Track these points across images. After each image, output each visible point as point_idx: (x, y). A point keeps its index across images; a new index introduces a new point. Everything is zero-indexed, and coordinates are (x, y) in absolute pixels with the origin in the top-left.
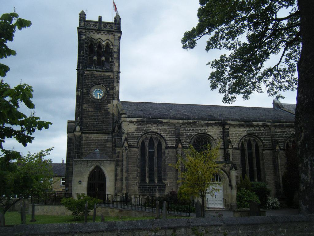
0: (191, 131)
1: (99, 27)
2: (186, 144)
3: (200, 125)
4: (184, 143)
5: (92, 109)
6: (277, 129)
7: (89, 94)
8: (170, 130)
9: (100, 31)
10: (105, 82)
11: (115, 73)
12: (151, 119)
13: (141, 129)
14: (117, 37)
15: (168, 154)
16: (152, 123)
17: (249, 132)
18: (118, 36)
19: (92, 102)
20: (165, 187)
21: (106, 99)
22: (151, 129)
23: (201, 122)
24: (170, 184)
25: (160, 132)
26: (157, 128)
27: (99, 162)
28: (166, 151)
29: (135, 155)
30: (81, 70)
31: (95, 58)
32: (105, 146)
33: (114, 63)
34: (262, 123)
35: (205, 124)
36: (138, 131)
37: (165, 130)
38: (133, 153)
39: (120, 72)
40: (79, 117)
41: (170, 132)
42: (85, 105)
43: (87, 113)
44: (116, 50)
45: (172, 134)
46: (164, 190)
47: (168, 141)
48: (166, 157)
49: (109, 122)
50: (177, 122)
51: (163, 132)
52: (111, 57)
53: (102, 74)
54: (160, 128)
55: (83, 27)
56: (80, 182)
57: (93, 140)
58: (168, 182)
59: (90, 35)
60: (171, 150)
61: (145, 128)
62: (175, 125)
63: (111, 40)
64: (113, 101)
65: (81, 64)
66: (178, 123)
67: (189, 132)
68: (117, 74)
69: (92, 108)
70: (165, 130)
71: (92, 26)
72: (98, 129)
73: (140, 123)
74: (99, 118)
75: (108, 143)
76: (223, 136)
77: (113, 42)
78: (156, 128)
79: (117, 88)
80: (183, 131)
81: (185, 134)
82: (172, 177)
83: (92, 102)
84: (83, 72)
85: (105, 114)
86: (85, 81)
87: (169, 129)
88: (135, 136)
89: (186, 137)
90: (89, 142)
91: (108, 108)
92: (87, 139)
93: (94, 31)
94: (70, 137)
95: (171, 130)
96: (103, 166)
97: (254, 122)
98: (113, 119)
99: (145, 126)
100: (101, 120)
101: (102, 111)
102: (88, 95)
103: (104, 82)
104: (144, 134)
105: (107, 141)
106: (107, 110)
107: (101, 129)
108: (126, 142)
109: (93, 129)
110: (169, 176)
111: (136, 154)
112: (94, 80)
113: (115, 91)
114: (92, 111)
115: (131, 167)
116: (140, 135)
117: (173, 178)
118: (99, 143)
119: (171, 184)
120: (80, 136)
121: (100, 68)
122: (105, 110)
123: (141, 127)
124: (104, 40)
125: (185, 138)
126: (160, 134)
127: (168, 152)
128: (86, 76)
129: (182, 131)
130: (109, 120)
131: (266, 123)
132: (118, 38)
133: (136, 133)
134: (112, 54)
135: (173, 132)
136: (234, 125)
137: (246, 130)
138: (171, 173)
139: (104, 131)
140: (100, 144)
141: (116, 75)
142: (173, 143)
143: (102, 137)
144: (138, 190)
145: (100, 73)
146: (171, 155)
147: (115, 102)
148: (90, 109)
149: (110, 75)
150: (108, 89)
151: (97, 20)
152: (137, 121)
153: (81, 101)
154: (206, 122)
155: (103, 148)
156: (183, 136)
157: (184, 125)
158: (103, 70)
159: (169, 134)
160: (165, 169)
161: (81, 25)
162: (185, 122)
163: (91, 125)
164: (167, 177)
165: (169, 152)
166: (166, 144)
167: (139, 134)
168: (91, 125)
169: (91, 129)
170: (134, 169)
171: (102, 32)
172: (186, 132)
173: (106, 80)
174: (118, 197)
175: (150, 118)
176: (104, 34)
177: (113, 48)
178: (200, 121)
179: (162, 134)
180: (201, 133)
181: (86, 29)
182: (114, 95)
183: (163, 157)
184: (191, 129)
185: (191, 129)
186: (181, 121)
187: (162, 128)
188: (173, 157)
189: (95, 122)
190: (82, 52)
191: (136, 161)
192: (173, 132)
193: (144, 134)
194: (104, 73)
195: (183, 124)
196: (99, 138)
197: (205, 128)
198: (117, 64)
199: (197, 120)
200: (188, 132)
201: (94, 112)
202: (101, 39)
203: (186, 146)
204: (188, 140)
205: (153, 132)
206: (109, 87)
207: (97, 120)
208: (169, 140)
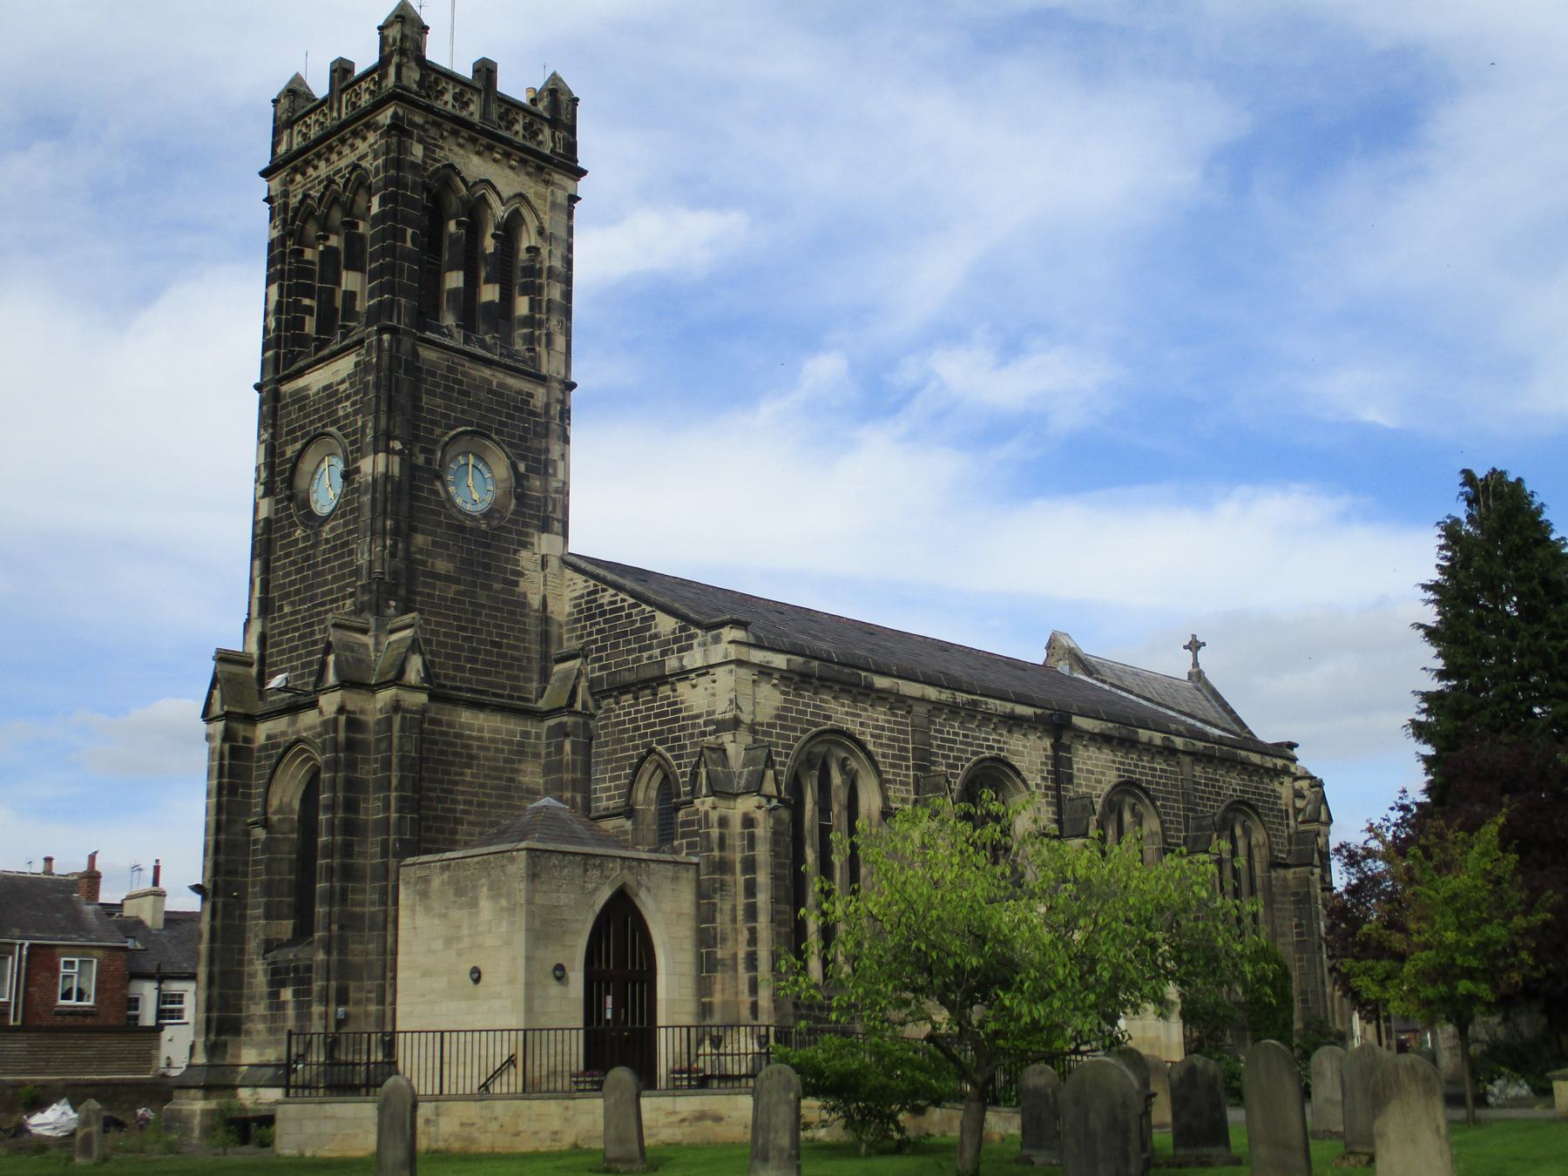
0: (962, 743)
1: (485, 115)
3: (987, 717)
5: (451, 566)
6: (1198, 770)
7: (439, 477)
8: (892, 730)
9: (487, 139)
10: (504, 424)
11: (555, 385)
12: (836, 667)
13: (798, 712)
14: (561, 197)
16: (837, 687)
17: (1125, 771)
18: (564, 188)
19: (450, 526)
21: (508, 522)
22: (828, 718)
23: (996, 705)
27: (630, 868)
30: (406, 333)
31: (454, 280)
32: (511, 780)
33: (549, 335)
34: (1163, 735)
36: (784, 718)
37: (875, 727)
39: (573, 386)
40: (393, 603)
42: (419, 539)
43: (426, 585)
44: (557, 263)
45: (901, 749)
49: (526, 649)
51: (872, 736)
52: (525, 291)
53: (495, 377)
54: (859, 716)
55: (416, 94)
56: (558, 973)
57: (459, 741)
59: (442, 148)
61: (808, 705)
63: (531, 197)
64: (540, 539)
65: (403, 301)
67: (951, 749)
68: (564, 394)
69: (451, 558)
70: (875, 727)
71: (448, 97)
72: (478, 682)
73: (797, 679)
74: (482, 623)
75: (523, 767)
76: (1057, 781)
77: (546, 218)
78: (847, 714)
79: (560, 465)
80: (936, 738)
81: (946, 757)
83: (450, 526)
84: (413, 345)
85: (505, 602)
86: (420, 399)
88: (777, 745)
90: (442, 752)
91: (521, 574)
92: (433, 732)
93: (465, 133)
94: (354, 712)
95: (900, 732)
96: (648, 889)
97: (1140, 730)
98: (545, 638)
100: (490, 634)
101: (497, 586)
102: (433, 484)
103: (502, 424)
104: (811, 738)
105: (520, 751)
106: (516, 584)
107: (490, 684)
108: (770, 773)
109: (454, 678)
112: (458, 402)
113: (555, 484)
114: (448, 579)
116: (796, 739)
118: (486, 758)
120: (424, 710)
121: (483, 345)
122: (506, 581)
123: (797, 703)
124: (505, 195)
126: (861, 745)
128: (420, 369)
130: (523, 641)
131: (1172, 737)
132: (566, 203)
133: (782, 727)
134: (538, 281)
136: (1087, 732)
137: (1114, 762)
139: (501, 696)
140: (490, 768)
141: (558, 401)
142: (904, 795)
143: (497, 731)
145: (487, 372)
147: (546, 543)
148: (442, 566)
149: (531, 395)
150: (522, 467)
151: (467, 72)
152: (789, 671)
153: (404, 508)
154: (1008, 706)
155: (508, 789)
158: (496, 358)
159: (888, 746)
161: (405, 82)
163: (448, 656)
167: (787, 737)
168: (448, 656)
169: (447, 677)
171: (500, 147)
172: (942, 747)
174: (725, 1055)
175: (833, 662)
176: (505, 161)
177: (544, 252)
178: (990, 700)
179: (871, 747)
181: (429, 109)
182: (550, 508)
186: (932, 693)
187: (869, 718)
189: (464, 638)
190: (409, 231)
194: (501, 376)
195: (937, 706)
196: (486, 735)
197: (1001, 735)
198: (559, 342)
199: (979, 695)
201: (457, 581)
202: (494, 188)
206: (523, 458)
207: (475, 630)
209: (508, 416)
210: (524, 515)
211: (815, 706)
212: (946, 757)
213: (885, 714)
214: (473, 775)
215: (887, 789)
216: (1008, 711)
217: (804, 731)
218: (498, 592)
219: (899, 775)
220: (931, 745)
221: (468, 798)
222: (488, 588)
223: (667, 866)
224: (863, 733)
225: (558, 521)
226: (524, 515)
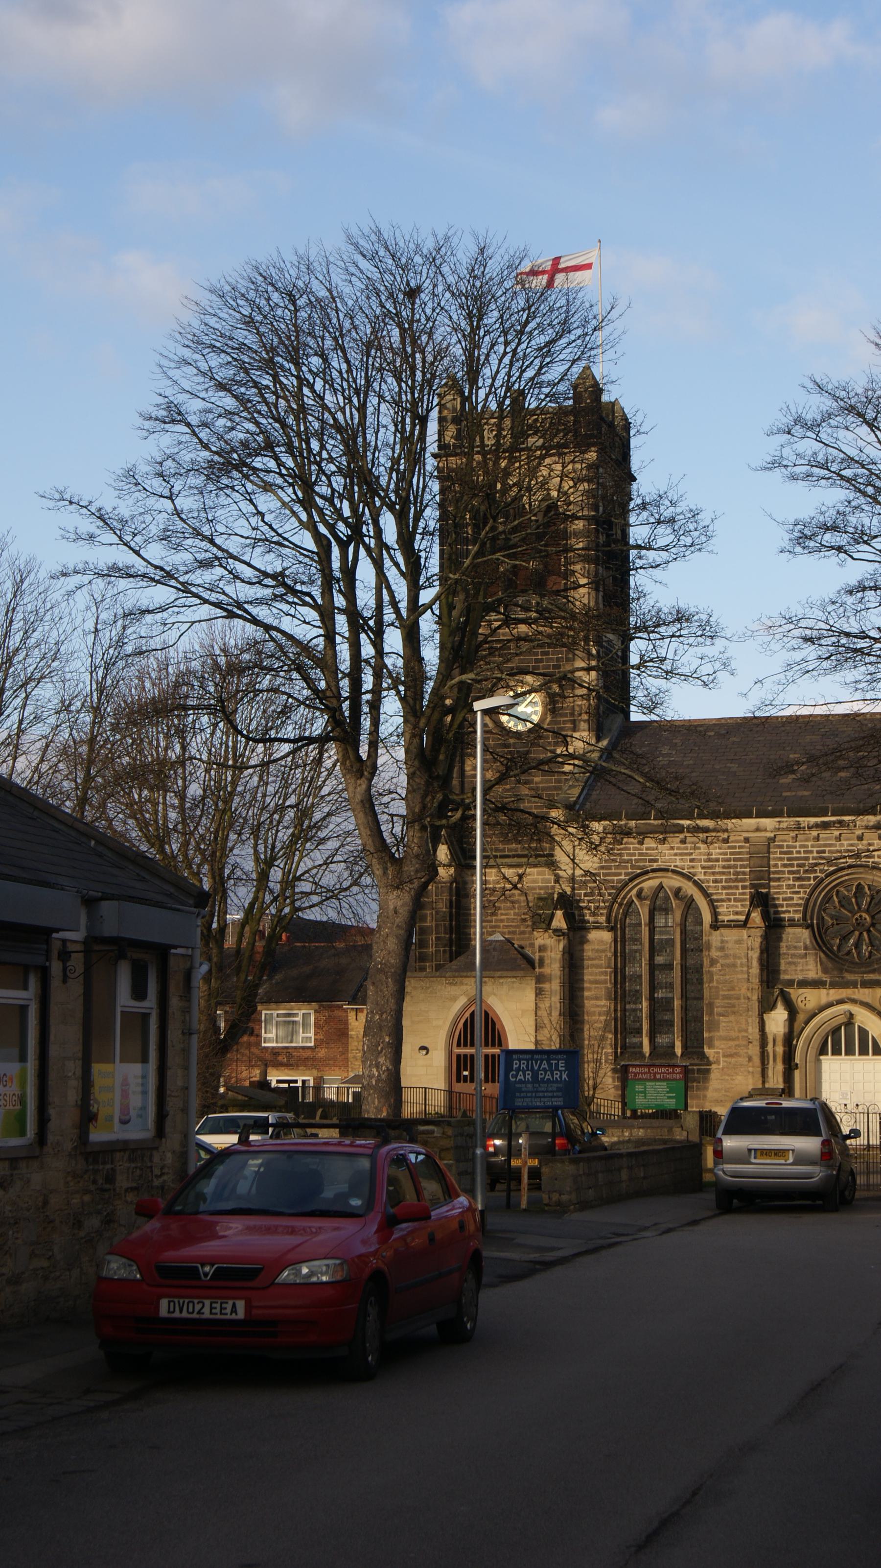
0: (814, 858)
2: (789, 912)
4: (782, 906)
8: (729, 860)
10: (541, 661)
15: (722, 949)
20: (708, 1071)
22: (656, 861)
24: (726, 1059)
25: (692, 870)
26: (681, 854)
28: (715, 938)
29: (600, 957)
35: (867, 827)
38: (593, 950)
41: (729, 867)
45: (737, 873)
46: (706, 1080)
47: (722, 900)
48: (713, 962)
50: (754, 827)
51: (703, 868)
54: (691, 854)
58: (718, 1053)
60: (730, 935)
61: (634, 855)
62: (747, 840)
66: (758, 830)
70: (709, 860)
78: (676, 855)
80: (781, 859)
81: (790, 872)
82: (733, 1034)
87: (726, 854)
89: (791, 882)
95: (735, 860)
99: (635, 849)
104: (631, 880)
109: (503, 850)
110: (722, 1033)
111: (604, 951)
115: (588, 998)
116: (619, 881)
117: (737, 1038)
119: (733, 1060)
125: (789, 887)
126: (688, 877)
127: (722, 942)
129: (777, 861)
135: (742, 866)
138: (732, 1018)
142: (740, 909)
144: (610, 1080)
146: (731, 952)
156: (778, 879)
157: (786, 837)
159: (723, 873)
160: (711, 1005)
162: (784, 825)
164: (717, 1034)
165: (727, 942)
166: (715, 914)
170: (598, 1006)
172: (792, 865)
173: (547, 653)
180: (850, 867)
183: (706, 962)
184: (811, 852)
185: (811, 852)
188: (739, 962)
191: (603, 977)
192: (742, 866)
193: (631, 880)
199: (833, 815)
200: (798, 865)
203: (791, 920)
204: (798, 893)
205: (666, 870)
208: (724, 897)
209: (543, 654)
210: (559, 723)
211: (640, 854)
212: (790, 872)
213: (720, 848)
214: (515, 914)
215: (717, 907)
216: (871, 824)
217: (626, 874)
218: (540, 783)
219: (735, 894)
220: (776, 866)
221: (512, 929)
222: (531, 782)
223: (514, 980)
224: (693, 867)
225: (585, 721)
226: (559, 723)
